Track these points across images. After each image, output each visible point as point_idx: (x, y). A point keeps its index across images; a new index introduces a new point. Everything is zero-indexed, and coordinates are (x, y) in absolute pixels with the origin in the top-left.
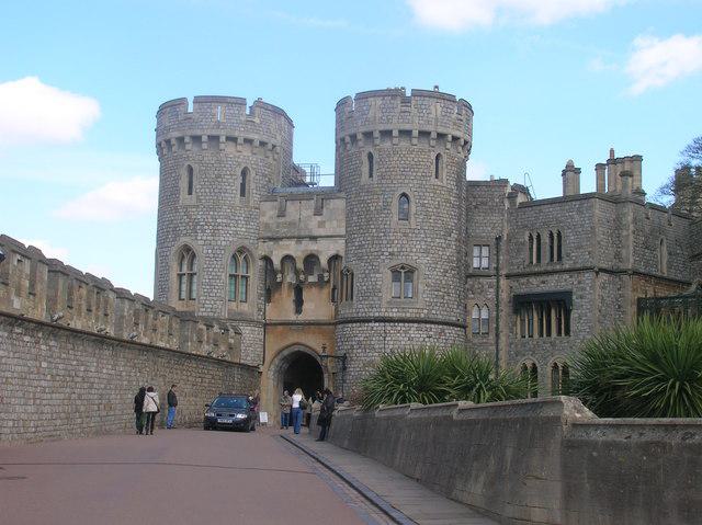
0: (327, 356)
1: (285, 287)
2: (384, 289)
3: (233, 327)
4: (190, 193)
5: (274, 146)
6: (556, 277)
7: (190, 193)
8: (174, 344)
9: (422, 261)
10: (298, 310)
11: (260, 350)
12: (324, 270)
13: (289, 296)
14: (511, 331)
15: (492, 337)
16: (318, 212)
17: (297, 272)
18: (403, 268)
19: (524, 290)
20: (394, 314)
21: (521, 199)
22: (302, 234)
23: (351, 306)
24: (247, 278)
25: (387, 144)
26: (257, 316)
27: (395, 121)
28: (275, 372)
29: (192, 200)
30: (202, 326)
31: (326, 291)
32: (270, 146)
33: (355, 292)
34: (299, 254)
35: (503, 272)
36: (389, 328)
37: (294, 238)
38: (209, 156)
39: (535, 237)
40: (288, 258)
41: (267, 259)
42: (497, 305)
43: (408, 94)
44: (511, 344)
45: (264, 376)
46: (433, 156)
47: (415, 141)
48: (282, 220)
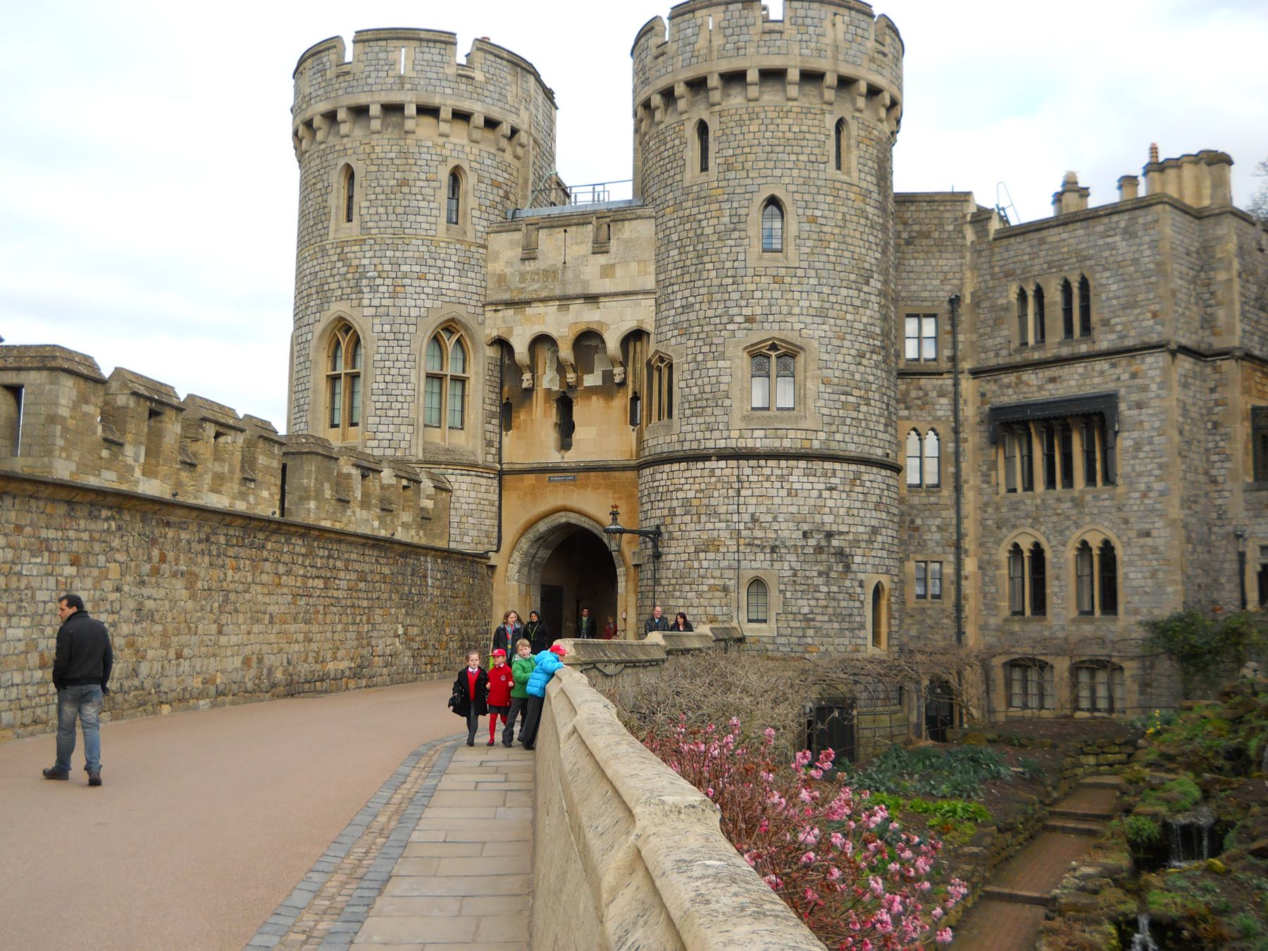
0: (622, 532)
1: (539, 397)
2: (735, 393)
3: (432, 477)
4: (349, 220)
5: (514, 131)
6: (1080, 368)
7: (349, 220)
8: (264, 503)
11: (491, 523)
12: (613, 362)
13: (546, 415)
14: (986, 478)
15: (947, 493)
16: (600, 247)
17: (561, 368)
18: (774, 347)
19: (1010, 397)
20: (758, 441)
21: (995, 225)
22: (571, 290)
23: (669, 427)
24: (463, 381)
25: (736, 99)
28: (522, 565)
29: (353, 230)
30: (346, 467)
31: (620, 402)
32: (505, 129)
35: (967, 365)
36: (748, 471)
39: (1030, 293)
40: (542, 341)
41: (502, 344)
42: (956, 431)
44: (986, 504)
46: (830, 122)
47: (793, 91)
48: (530, 266)
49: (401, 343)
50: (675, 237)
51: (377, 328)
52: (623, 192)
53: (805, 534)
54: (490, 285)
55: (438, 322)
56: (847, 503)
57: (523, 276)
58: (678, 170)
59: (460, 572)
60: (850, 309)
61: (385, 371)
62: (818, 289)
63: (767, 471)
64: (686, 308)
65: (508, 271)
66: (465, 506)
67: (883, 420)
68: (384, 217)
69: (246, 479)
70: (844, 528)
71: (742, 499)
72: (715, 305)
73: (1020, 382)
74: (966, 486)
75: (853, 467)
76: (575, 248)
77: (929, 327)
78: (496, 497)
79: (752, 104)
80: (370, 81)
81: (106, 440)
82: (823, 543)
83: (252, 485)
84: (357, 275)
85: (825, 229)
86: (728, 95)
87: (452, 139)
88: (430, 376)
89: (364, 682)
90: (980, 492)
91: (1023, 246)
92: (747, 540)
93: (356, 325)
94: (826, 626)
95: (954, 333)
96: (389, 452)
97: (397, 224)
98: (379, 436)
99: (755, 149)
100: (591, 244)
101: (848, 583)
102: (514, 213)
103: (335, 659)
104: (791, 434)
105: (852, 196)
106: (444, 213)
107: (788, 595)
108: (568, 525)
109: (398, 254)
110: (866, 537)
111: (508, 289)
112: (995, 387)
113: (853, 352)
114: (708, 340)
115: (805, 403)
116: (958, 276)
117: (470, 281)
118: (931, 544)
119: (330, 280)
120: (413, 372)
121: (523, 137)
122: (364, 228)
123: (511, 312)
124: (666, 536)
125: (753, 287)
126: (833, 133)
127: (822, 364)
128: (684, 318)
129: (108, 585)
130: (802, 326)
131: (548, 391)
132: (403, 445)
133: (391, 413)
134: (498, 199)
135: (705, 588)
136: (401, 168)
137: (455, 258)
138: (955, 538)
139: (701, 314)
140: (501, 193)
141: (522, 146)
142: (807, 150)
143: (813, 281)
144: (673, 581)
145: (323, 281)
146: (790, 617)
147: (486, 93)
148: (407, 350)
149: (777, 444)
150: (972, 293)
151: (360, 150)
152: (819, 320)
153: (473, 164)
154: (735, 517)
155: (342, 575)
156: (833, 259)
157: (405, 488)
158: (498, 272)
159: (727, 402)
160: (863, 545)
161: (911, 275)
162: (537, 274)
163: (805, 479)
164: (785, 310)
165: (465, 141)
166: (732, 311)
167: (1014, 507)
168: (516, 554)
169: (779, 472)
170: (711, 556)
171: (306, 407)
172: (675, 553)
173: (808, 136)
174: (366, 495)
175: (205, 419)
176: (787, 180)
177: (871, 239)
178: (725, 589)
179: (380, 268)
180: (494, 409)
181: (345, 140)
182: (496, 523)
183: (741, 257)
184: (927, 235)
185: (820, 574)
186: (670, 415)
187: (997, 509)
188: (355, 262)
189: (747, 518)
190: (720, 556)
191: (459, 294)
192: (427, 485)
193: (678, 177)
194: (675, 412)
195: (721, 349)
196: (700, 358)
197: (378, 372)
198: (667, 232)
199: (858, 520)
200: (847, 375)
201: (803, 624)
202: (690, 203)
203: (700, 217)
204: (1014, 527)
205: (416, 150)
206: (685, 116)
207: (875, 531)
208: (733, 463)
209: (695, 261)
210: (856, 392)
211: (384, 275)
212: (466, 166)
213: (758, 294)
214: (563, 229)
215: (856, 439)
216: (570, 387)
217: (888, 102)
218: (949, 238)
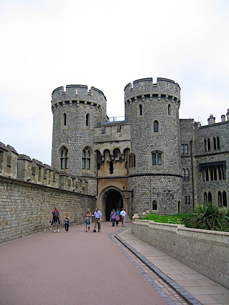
1: (106, 162)
3: (84, 180)
4: (65, 125)
5: (99, 106)
7: (65, 125)
8: (57, 186)
9: (164, 149)
10: (111, 172)
13: (107, 166)
14: (199, 178)
15: (191, 181)
16: (119, 131)
17: (110, 156)
18: (157, 152)
19: (203, 162)
20: (154, 172)
22: (113, 140)
23: (135, 170)
24: (89, 159)
25: (148, 100)
26: (94, 175)
27: (151, 90)
28: (102, 199)
29: (66, 126)
31: (123, 164)
32: (98, 106)
35: (194, 155)
36: (152, 178)
38: (73, 109)
39: (207, 140)
40: (106, 151)
41: (98, 151)
42: (192, 169)
44: (199, 184)
46: (167, 105)
47: (160, 99)
48: (103, 135)
49: (77, 151)
50: (135, 129)
51: (72, 148)
53: (164, 191)
54: (95, 139)
55: (84, 147)
56: (173, 184)
57: (102, 137)
58: (135, 115)
59: (91, 200)
60: (172, 144)
61: (74, 157)
63: (156, 178)
65: (99, 136)
66: (91, 186)
67: (179, 167)
68: (73, 124)
69: (54, 181)
70: (172, 190)
71: (151, 184)
72: (144, 143)
73: (205, 158)
74: (194, 180)
75: (174, 177)
76: (113, 131)
78: (97, 184)
79: (151, 101)
80: (69, 96)
81: (32, 174)
82: (168, 193)
83: (55, 182)
84: (67, 137)
85: (167, 127)
86: (146, 99)
87: (87, 108)
88: (83, 158)
89: (76, 224)
90: (197, 181)
91: (205, 130)
92: (152, 193)
93: (67, 148)
94: (169, 210)
95: (191, 148)
96: (75, 174)
97: (76, 126)
98: (73, 171)
99: (152, 111)
100: (117, 130)
101: (173, 201)
102: (99, 123)
103: (71, 219)
104: (161, 170)
105: (172, 120)
106: (85, 124)
107: (161, 204)
108: (112, 189)
109: (76, 132)
110: (176, 191)
111: (99, 140)
112: (200, 160)
113: (173, 153)
114: (143, 151)
115: (164, 164)
116: (192, 136)
117: (91, 138)
119: (61, 138)
120: (80, 158)
121: (101, 107)
122: (68, 127)
123: (99, 144)
124: (135, 192)
125: (152, 139)
126: (168, 107)
127: (167, 155)
128: (138, 146)
129: (37, 204)
130: (163, 147)
131: (108, 161)
132: (78, 173)
133: (75, 166)
134: (96, 120)
135: (144, 203)
136: (76, 114)
137: (88, 133)
138: (192, 191)
139: (141, 145)
140: (97, 119)
141: (101, 109)
142: (163, 111)
143: (165, 138)
144: (136, 201)
145: (60, 138)
146: (162, 208)
147: (94, 98)
148: (78, 153)
149: (158, 172)
150: (195, 140)
151: (68, 110)
152: (166, 146)
153: (91, 113)
154: (150, 188)
155: (72, 201)
156: (168, 134)
157: (80, 182)
158: (97, 136)
159: (147, 164)
160: (176, 193)
161: (182, 136)
162: (105, 136)
163: (164, 179)
164: (159, 144)
165: (89, 108)
166: (148, 144)
167: (205, 184)
168: (101, 196)
169: (158, 178)
170: (145, 196)
171: (56, 165)
172: (136, 195)
173: (163, 108)
174: (73, 184)
175: (48, 169)
176: (159, 117)
177: (176, 129)
178: (148, 203)
179: (72, 135)
180: (96, 165)
181: (64, 108)
182: (97, 189)
183: (150, 133)
184: (185, 128)
185: (168, 199)
186: (135, 166)
187: (201, 185)
188: (67, 134)
189: (152, 188)
190: (147, 196)
191: (89, 141)
192: (84, 182)
193: (135, 116)
194: (136, 166)
195: (146, 152)
196: (141, 154)
197: (72, 157)
198: (133, 128)
199: (175, 188)
200: (172, 158)
201: (164, 210)
202: (138, 122)
203: (141, 125)
204: (205, 188)
205: (79, 110)
206: (137, 104)
207: (178, 190)
208: (149, 176)
209: (140, 134)
210: (174, 161)
211: (73, 137)
212: (90, 114)
213: (153, 141)
214: (110, 127)
215: (174, 171)
216: (112, 160)
217: (178, 101)
218: (190, 129)
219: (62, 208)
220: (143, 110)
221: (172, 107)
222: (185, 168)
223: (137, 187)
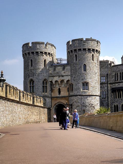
4: (32, 66)
5: (52, 54)
7: (32, 66)
14: (111, 97)
15: (106, 99)
16: (64, 69)
17: (59, 84)
18: (85, 82)
21: (112, 65)
24: (46, 87)
25: (80, 52)
26: (50, 96)
27: (82, 46)
32: (51, 54)
33: (74, 89)
34: (59, 80)
35: (109, 83)
36: (82, 97)
37: (58, 76)
40: (56, 81)
41: (51, 82)
42: (108, 91)
43: (84, 39)
44: (111, 100)
45: (52, 110)
50: (73, 69)
52: (65, 62)
62: (90, 75)
64: (75, 78)
77: (104, 78)
90: (111, 98)
95: (107, 79)
108: (59, 104)
118: (105, 105)
122: (34, 67)
159: (80, 89)
186: (73, 91)
189: (82, 103)
193: (73, 61)
194: (73, 90)
207: (97, 104)
210: (95, 87)
213: (83, 76)
219: (35, 114)
220: (77, 58)
221: (94, 56)
222: (104, 91)
223: (74, 102)
